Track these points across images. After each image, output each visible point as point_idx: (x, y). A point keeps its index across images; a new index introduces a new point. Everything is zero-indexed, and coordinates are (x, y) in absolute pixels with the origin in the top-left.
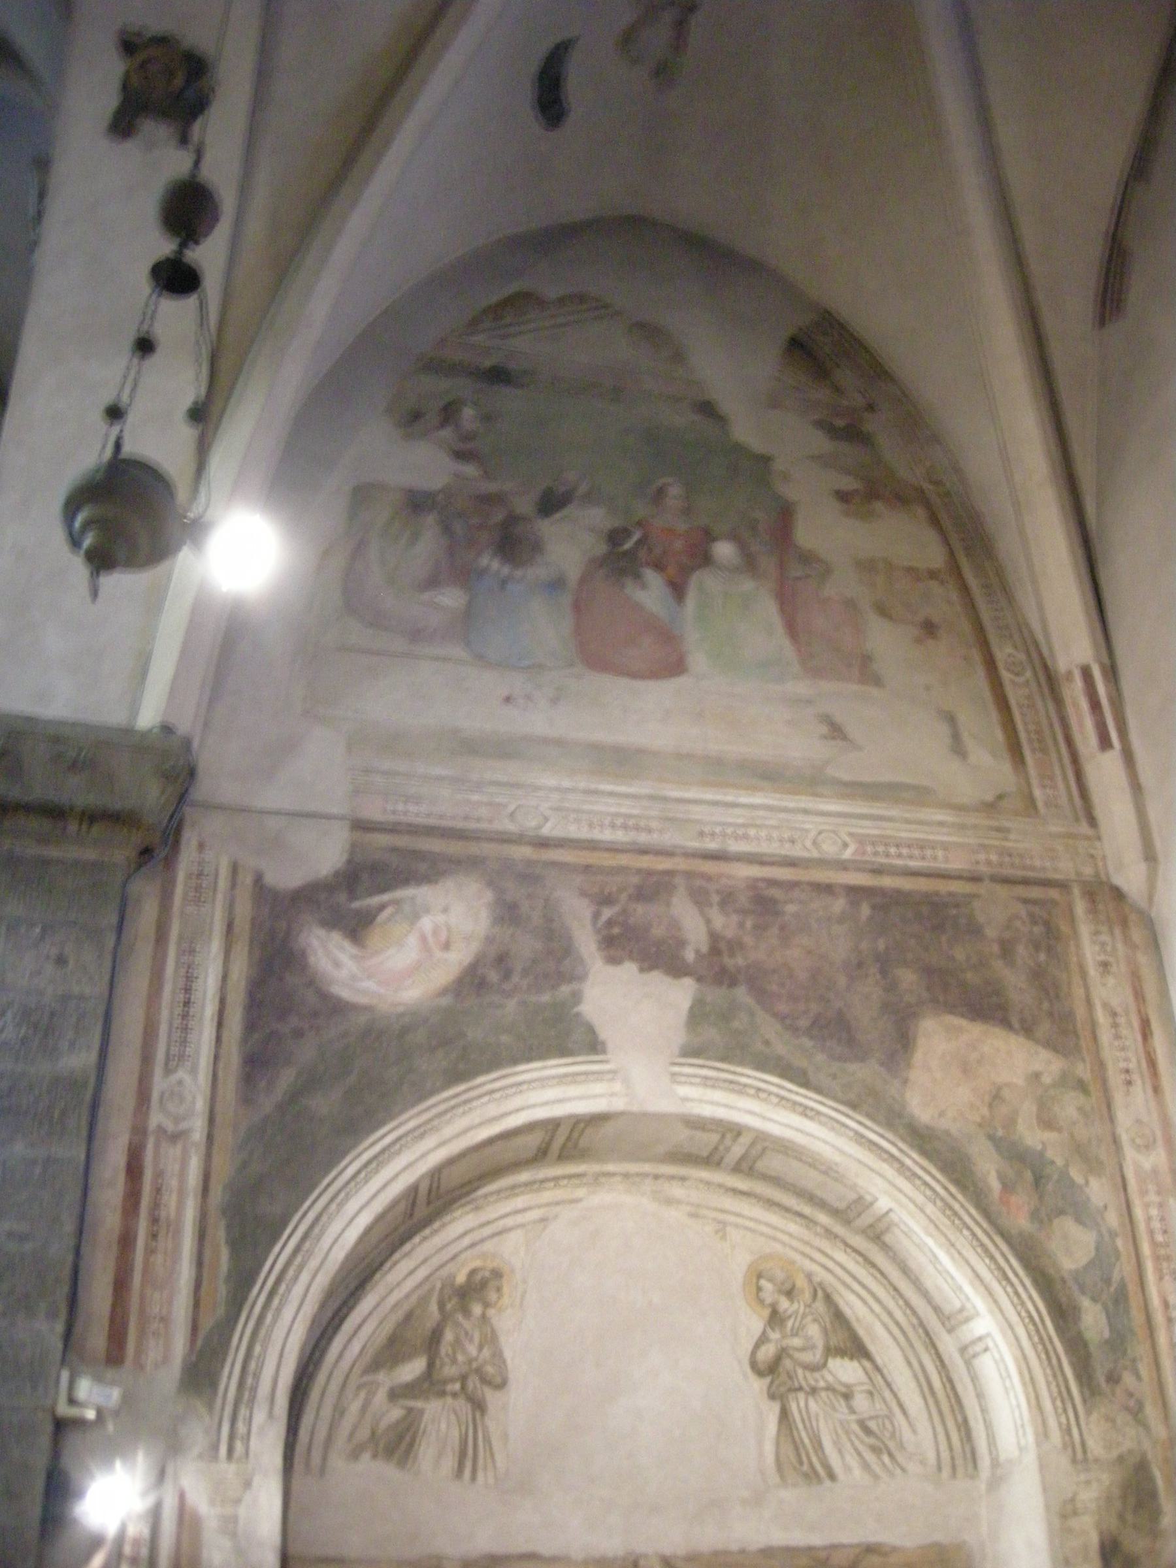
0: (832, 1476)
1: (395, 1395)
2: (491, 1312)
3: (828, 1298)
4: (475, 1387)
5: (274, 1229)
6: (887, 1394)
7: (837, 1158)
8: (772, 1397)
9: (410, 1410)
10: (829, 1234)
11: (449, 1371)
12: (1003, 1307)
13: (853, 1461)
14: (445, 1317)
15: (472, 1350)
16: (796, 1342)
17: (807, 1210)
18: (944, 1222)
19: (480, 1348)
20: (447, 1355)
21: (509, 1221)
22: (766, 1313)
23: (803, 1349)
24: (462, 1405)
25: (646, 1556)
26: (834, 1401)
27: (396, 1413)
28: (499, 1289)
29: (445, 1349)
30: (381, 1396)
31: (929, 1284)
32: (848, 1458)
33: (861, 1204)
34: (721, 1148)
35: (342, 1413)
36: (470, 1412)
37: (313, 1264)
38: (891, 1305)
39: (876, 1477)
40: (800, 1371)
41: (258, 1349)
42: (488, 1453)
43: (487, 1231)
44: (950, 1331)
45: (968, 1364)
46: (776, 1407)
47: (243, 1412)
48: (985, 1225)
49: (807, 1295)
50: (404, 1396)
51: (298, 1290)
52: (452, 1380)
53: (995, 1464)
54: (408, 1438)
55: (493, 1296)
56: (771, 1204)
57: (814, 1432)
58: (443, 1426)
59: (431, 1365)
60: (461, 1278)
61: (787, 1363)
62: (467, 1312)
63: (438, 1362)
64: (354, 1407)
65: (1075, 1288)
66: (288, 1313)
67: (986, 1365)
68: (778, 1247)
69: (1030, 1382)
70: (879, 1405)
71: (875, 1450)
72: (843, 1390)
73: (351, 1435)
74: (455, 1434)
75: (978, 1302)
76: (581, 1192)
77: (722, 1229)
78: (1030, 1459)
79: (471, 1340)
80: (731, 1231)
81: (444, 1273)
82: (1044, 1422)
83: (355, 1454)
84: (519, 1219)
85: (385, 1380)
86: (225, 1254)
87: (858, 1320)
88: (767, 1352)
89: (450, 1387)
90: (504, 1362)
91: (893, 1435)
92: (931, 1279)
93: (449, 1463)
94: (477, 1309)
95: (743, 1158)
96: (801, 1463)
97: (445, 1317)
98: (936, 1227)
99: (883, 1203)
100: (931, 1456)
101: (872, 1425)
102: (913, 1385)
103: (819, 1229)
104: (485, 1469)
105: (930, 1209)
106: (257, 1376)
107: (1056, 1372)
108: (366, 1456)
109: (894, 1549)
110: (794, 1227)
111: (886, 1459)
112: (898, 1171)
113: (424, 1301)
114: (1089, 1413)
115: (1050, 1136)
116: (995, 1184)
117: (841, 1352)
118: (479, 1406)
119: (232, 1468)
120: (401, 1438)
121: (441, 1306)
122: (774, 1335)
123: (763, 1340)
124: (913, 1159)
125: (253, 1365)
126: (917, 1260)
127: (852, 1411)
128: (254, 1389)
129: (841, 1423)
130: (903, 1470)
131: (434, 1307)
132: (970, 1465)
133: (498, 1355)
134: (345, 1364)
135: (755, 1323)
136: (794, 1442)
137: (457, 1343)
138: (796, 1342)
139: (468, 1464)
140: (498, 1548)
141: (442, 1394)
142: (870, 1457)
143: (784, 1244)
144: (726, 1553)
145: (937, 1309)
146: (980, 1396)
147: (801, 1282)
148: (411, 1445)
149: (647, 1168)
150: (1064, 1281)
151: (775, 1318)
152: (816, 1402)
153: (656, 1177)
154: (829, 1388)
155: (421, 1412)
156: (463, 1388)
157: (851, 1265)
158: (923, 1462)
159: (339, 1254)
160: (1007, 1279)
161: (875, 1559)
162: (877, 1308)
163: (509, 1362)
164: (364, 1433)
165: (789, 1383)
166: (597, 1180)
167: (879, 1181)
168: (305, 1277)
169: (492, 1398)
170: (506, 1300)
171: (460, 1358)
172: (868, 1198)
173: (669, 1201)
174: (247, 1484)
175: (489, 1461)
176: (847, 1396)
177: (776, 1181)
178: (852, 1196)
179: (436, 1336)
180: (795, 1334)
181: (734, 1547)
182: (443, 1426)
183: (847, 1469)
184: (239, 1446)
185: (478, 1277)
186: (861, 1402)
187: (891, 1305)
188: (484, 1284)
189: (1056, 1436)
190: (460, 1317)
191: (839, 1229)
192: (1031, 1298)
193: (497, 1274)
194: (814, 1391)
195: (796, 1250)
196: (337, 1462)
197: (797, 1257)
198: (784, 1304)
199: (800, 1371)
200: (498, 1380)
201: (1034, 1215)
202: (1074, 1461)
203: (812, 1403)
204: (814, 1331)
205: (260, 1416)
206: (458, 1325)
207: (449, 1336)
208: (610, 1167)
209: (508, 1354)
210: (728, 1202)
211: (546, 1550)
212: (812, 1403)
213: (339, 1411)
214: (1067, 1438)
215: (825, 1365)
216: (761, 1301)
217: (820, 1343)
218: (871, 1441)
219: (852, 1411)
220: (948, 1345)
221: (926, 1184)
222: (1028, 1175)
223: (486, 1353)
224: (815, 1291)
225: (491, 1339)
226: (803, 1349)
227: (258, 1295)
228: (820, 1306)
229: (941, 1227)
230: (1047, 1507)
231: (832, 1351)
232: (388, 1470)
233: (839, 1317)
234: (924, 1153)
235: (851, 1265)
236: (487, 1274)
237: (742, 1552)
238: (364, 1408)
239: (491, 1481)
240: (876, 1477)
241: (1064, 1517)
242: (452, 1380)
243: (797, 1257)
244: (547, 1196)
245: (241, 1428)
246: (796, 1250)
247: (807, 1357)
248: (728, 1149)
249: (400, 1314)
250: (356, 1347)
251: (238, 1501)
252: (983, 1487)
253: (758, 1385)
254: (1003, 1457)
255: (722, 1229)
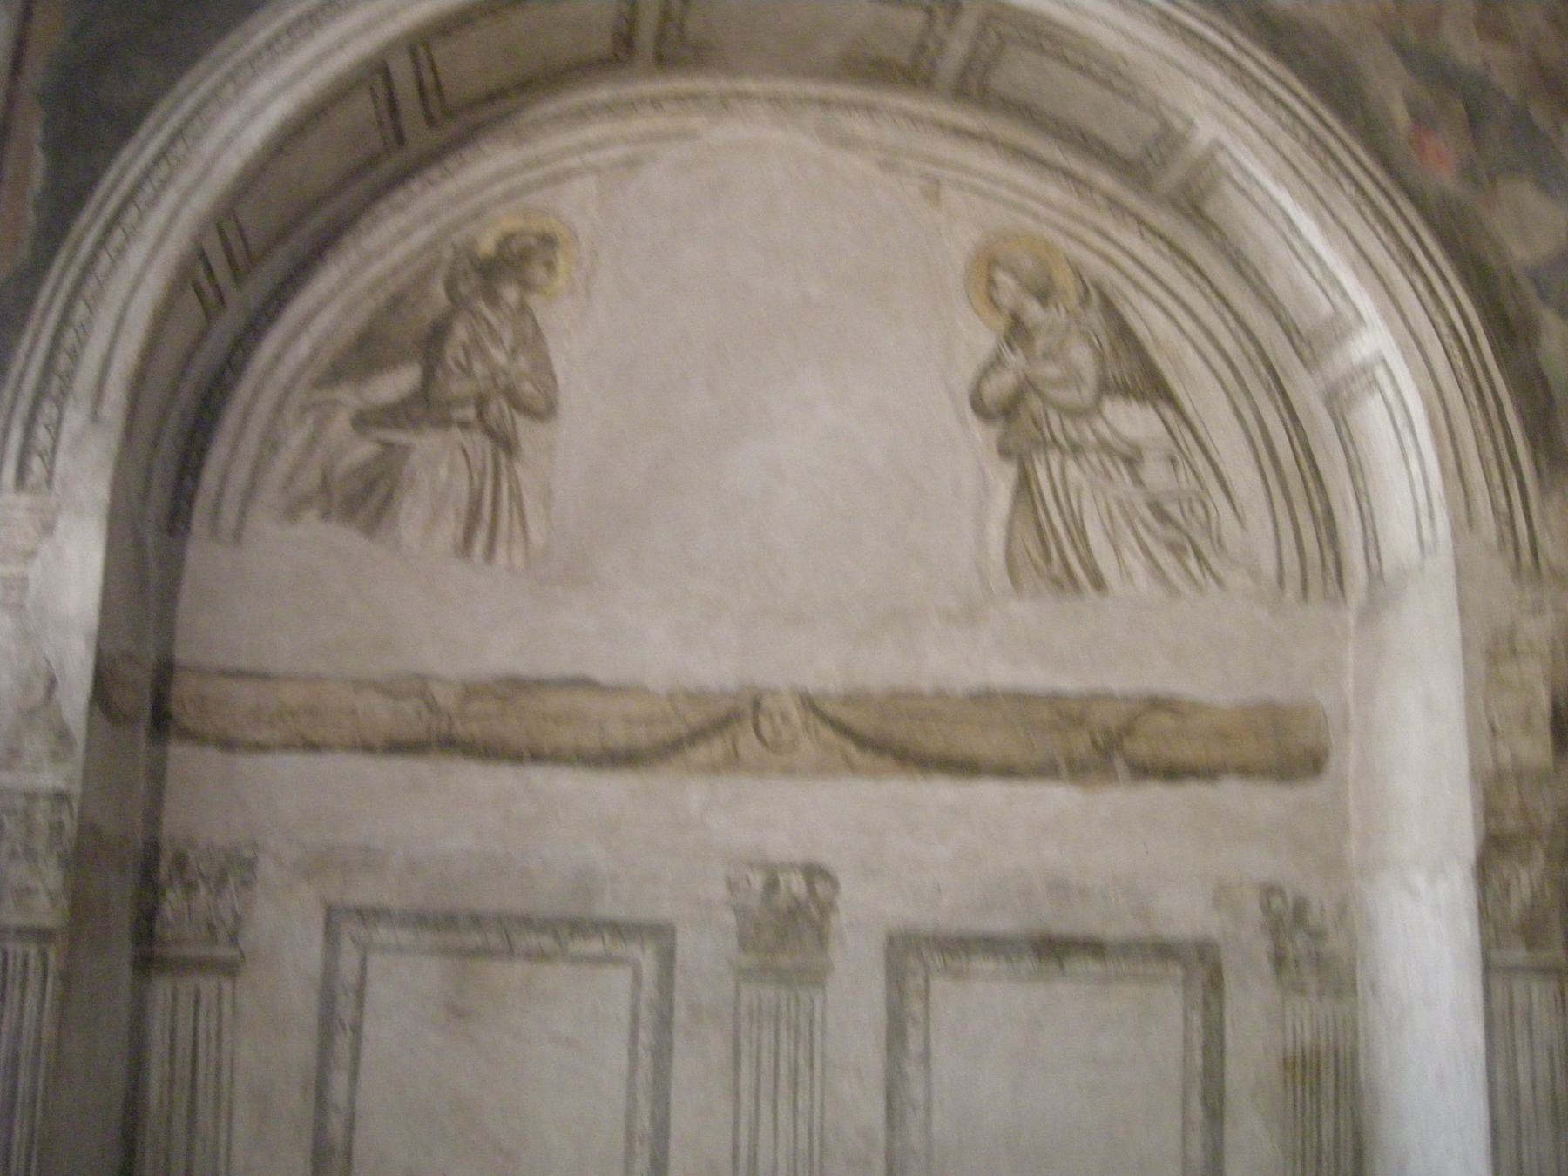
0: (1099, 583)
1: (364, 422)
2: (534, 301)
3: (1108, 306)
4: (501, 410)
5: (125, 125)
6: (1200, 462)
7: (1126, 48)
8: (1004, 452)
9: (388, 446)
10: (1114, 204)
11: (458, 387)
12: (1405, 306)
13: (1136, 563)
14: (457, 303)
15: (499, 356)
16: (1052, 371)
17: (1077, 165)
18: (1309, 166)
19: (513, 354)
20: (458, 363)
21: (573, 162)
22: (1001, 323)
23: (1063, 383)
24: (478, 443)
25: (775, 693)
26: (1109, 465)
27: (364, 450)
28: (550, 266)
29: (453, 351)
30: (341, 423)
31: (1279, 285)
32: (1128, 558)
33: (1169, 140)
34: (931, 45)
35: (275, 448)
36: (488, 451)
37: (185, 178)
38: (1212, 321)
39: (1173, 591)
40: (1054, 419)
41: (81, 309)
42: (516, 516)
43: (535, 174)
44: (1310, 362)
45: (1340, 421)
46: (1011, 471)
47: (48, 409)
48: (1379, 174)
49: (1073, 300)
50: (379, 424)
51: (157, 218)
52: (462, 402)
53: (1375, 575)
54: (382, 490)
55: (538, 273)
56: (1018, 154)
57: (1073, 514)
58: (443, 473)
59: (428, 376)
60: (487, 245)
61: (1035, 403)
62: (493, 299)
63: (439, 373)
64: (296, 440)
65: (1530, 290)
66: (136, 255)
67: (1372, 417)
68: (1028, 223)
69: (1447, 435)
70: (1184, 474)
71: (1174, 548)
72: (1124, 448)
73: (291, 479)
74: (462, 485)
75: (1366, 303)
76: (697, 122)
77: (933, 191)
78: (1442, 563)
79: (498, 341)
80: (951, 196)
81: (457, 238)
82: (1468, 506)
83: (292, 513)
84: (591, 158)
85: (349, 398)
86: (39, 160)
87: (1155, 340)
88: (1001, 385)
89: (458, 414)
90: (552, 375)
91: (1207, 528)
92: (1286, 276)
93: (449, 530)
94: (510, 294)
95: (968, 66)
96: (1047, 557)
97: (457, 303)
98: (1293, 167)
99: (1206, 131)
100: (1268, 565)
101: (1173, 510)
102: (1243, 447)
103: (1098, 198)
104: (511, 538)
105: (1285, 141)
106: (75, 356)
107: (1494, 422)
108: (311, 516)
109: (1197, 707)
110: (1054, 191)
111: (1192, 563)
112: (1233, 79)
113: (424, 277)
114: (1544, 490)
115: (1498, 54)
116: (1400, 115)
117: (1125, 391)
118: (506, 444)
119: (24, 500)
120: (370, 485)
121: (451, 287)
122: (1015, 359)
123: (996, 362)
124: (1259, 61)
125: (70, 337)
126: (1259, 236)
127: (1138, 481)
128: (69, 377)
129: (1120, 503)
130: (1219, 582)
131: (439, 290)
132: (1332, 586)
133: (543, 367)
134: (283, 374)
135: (981, 338)
136: (1038, 525)
137: (475, 346)
138: (1052, 371)
139: (481, 537)
140: (522, 666)
141: (444, 423)
142: (1165, 559)
143: (1036, 216)
144: (914, 695)
145: (1290, 331)
146: (1356, 469)
147: (1064, 278)
148: (389, 498)
149: (812, 88)
150: (1513, 279)
151: (1017, 331)
152: (1079, 465)
153: (825, 103)
154: (1105, 446)
155: (407, 450)
156: (481, 415)
157: (1151, 258)
158: (1255, 573)
159: (232, 163)
160: (1414, 262)
161: (1165, 721)
162: (1188, 324)
163: (561, 380)
164: (310, 479)
165: (1034, 432)
166: (724, 104)
167: (1199, 93)
168: (170, 197)
169: (527, 432)
170: (560, 282)
171: (478, 368)
172: (1178, 124)
173: (848, 142)
174: (48, 528)
175: (517, 530)
176: (1132, 460)
177: (1024, 111)
178: (1151, 126)
179: (438, 333)
180: (1048, 355)
181: (926, 685)
182: (443, 473)
183: (1126, 573)
184: (36, 464)
185: (515, 247)
186: (1155, 473)
187: (1212, 321)
188: (525, 256)
189: (1488, 526)
190: (483, 307)
191: (1131, 200)
192: (1454, 296)
193: (548, 241)
194: (1076, 449)
195: (1059, 229)
196: (263, 521)
197: (1061, 241)
198: (1033, 311)
199: (1054, 419)
200: (541, 404)
201: (1468, 172)
202: (1517, 569)
203: (1073, 470)
204: (1082, 356)
205: (75, 419)
206: (475, 314)
207: (461, 332)
208: (749, 85)
209: (559, 365)
210: (946, 148)
211: (601, 674)
212: (1073, 470)
213: (271, 442)
214: (1506, 529)
215: (1096, 408)
216: (995, 305)
217: (1089, 372)
218: (1172, 534)
219: (1138, 481)
220: (1306, 390)
221: (1277, 100)
222: (1459, 108)
223: (523, 363)
224: (1086, 290)
225: (532, 340)
226: (1063, 383)
227: (87, 228)
228: (1094, 318)
229: (1302, 169)
230: (1466, 642)
231: (1106, 387)
232: (346, 537)
233: (1123, 333)
234: (1276, 51)
235: (1151, 258)
236: (532, 241)
237: (941, 695)
238: (312, 442)
239: (519, 560)
240: (1173, 591)
241: (1492, 658)
242: (462, 402)
243: (1061, 241)
244: (640, 124)
245: (42, 435)
246: (1059, 229)
247: (1068, 396)
248: (941, 45)
249: (382, 297)
250: (304, 347)
251: (29, 555)
252: (1351, 618)
253: (982, 436)
254: (1387, 567)
255: (933, 191)
